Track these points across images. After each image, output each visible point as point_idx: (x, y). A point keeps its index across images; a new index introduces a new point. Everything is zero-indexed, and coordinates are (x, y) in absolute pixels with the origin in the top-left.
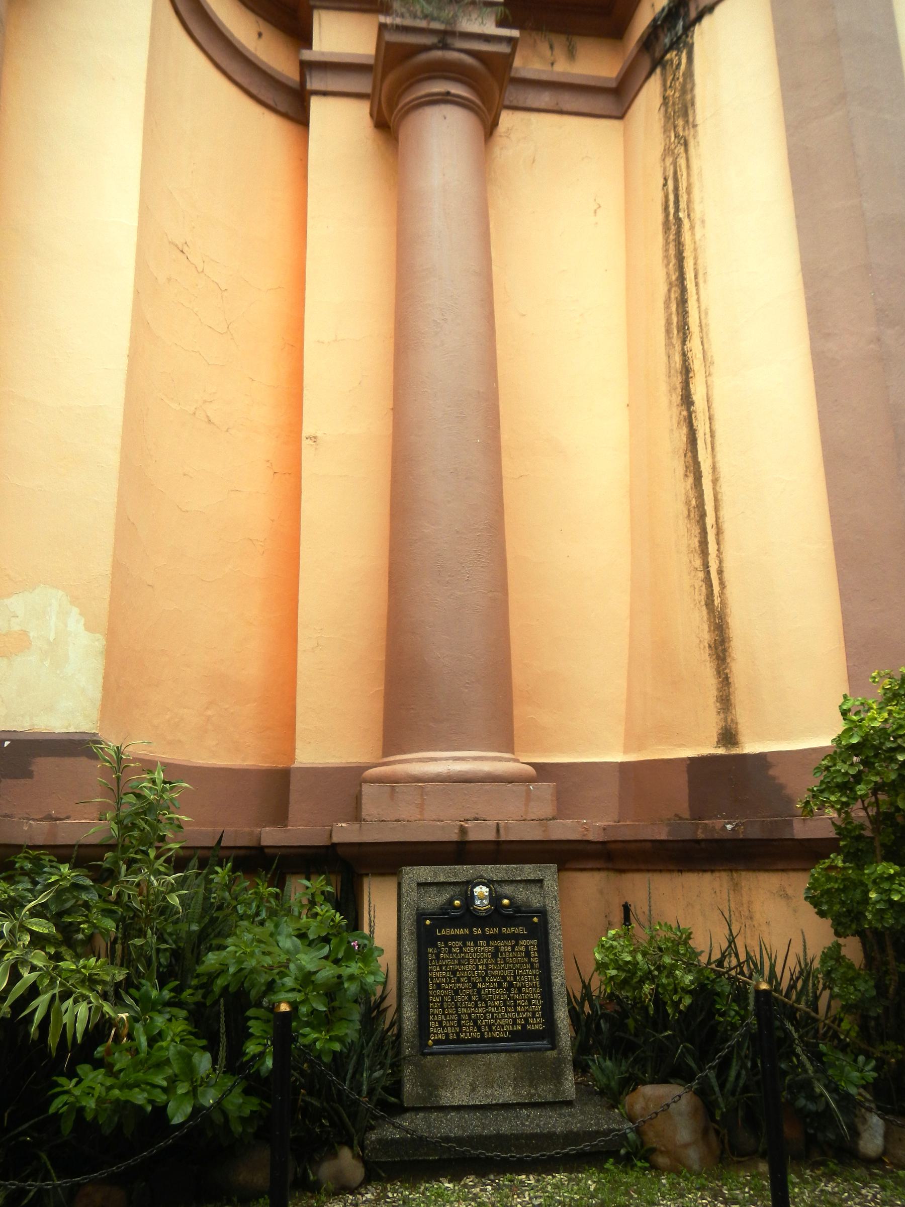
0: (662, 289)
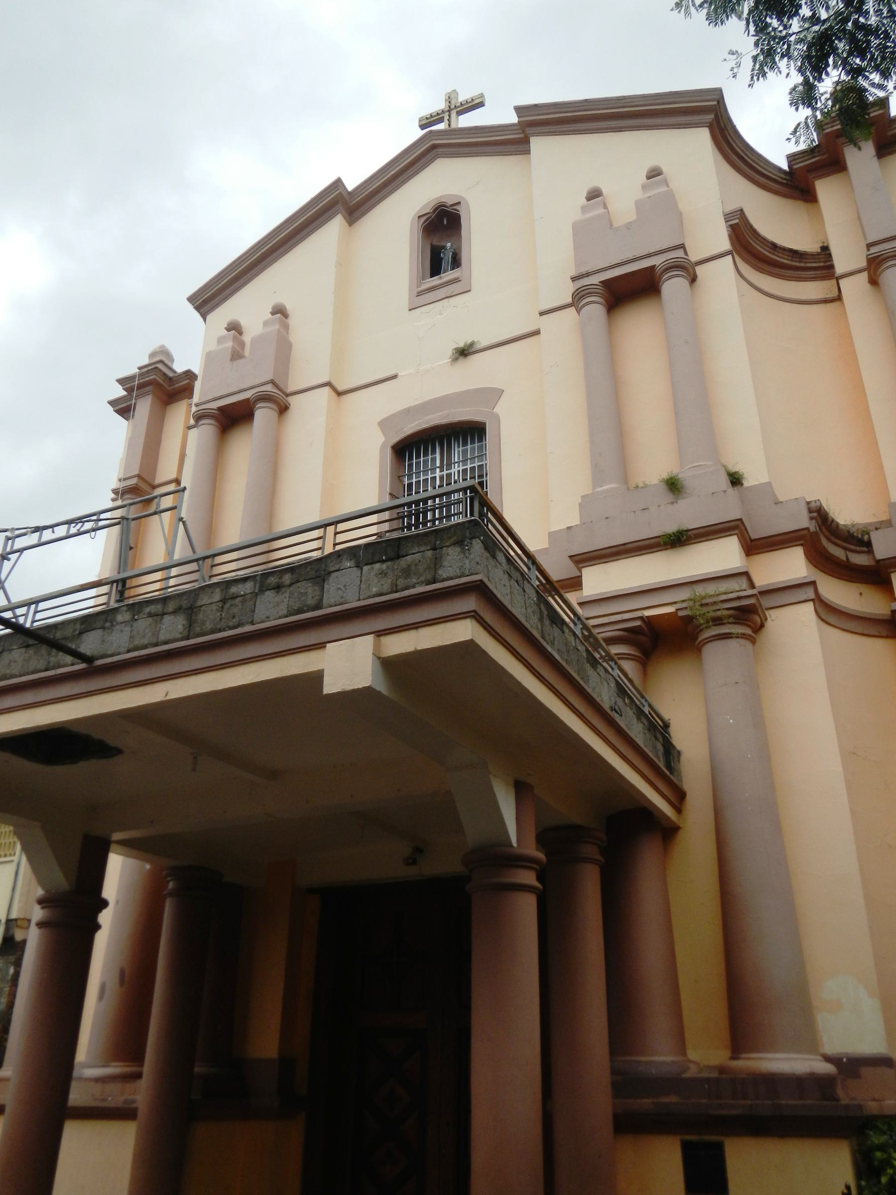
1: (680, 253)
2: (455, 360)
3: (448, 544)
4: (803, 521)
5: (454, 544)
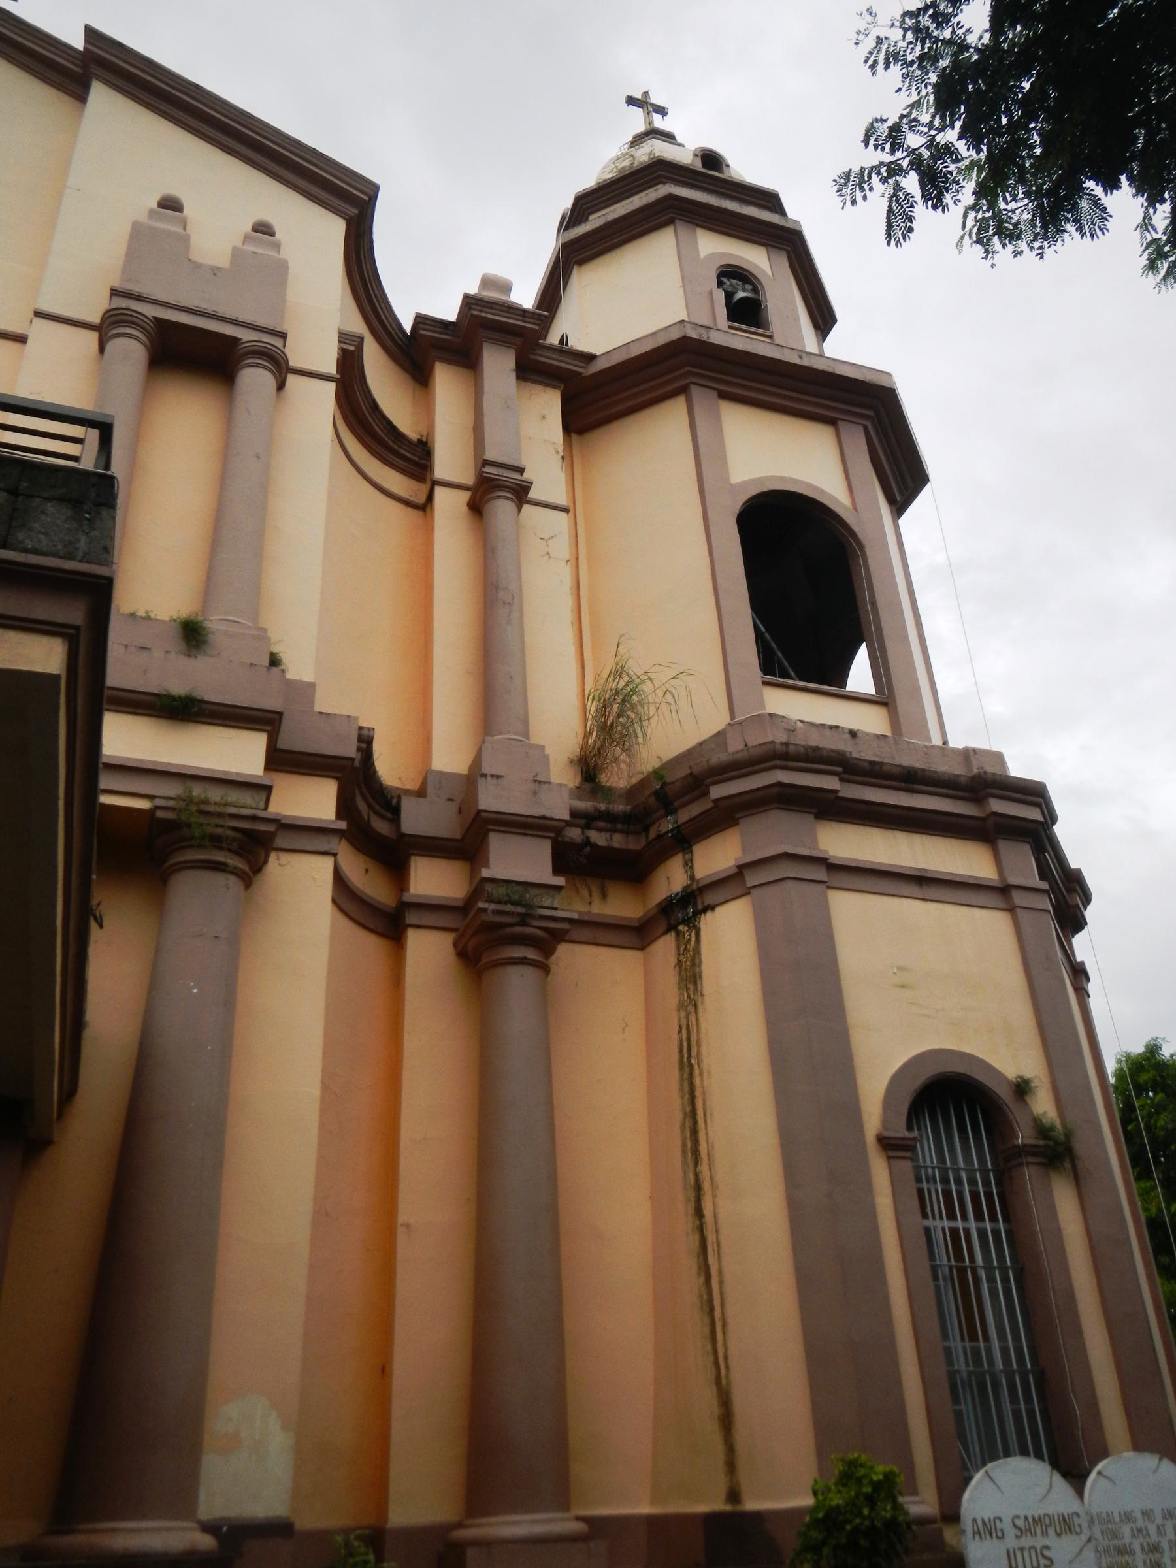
0: (678, 1116)
1: (278, 342)
3: (45, 495)
4: (350, 750)
5: (62, 500)
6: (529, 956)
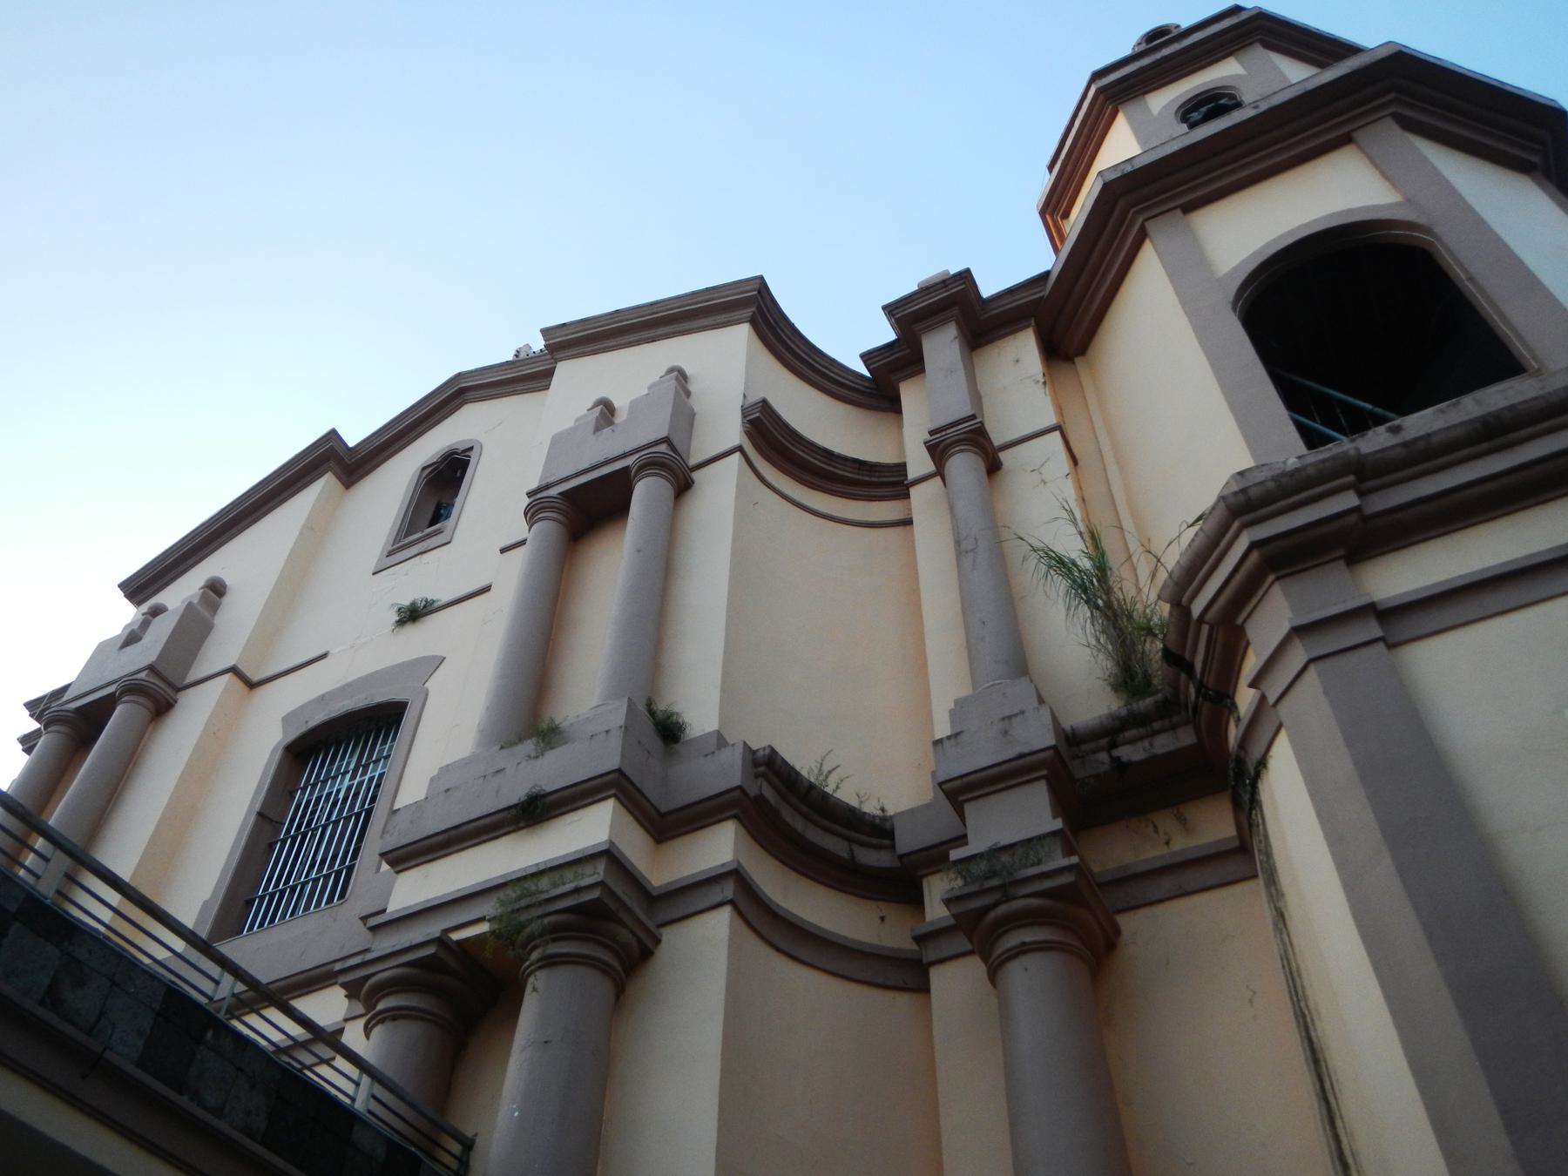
2: (401, 623)
6: (1028, 939)
